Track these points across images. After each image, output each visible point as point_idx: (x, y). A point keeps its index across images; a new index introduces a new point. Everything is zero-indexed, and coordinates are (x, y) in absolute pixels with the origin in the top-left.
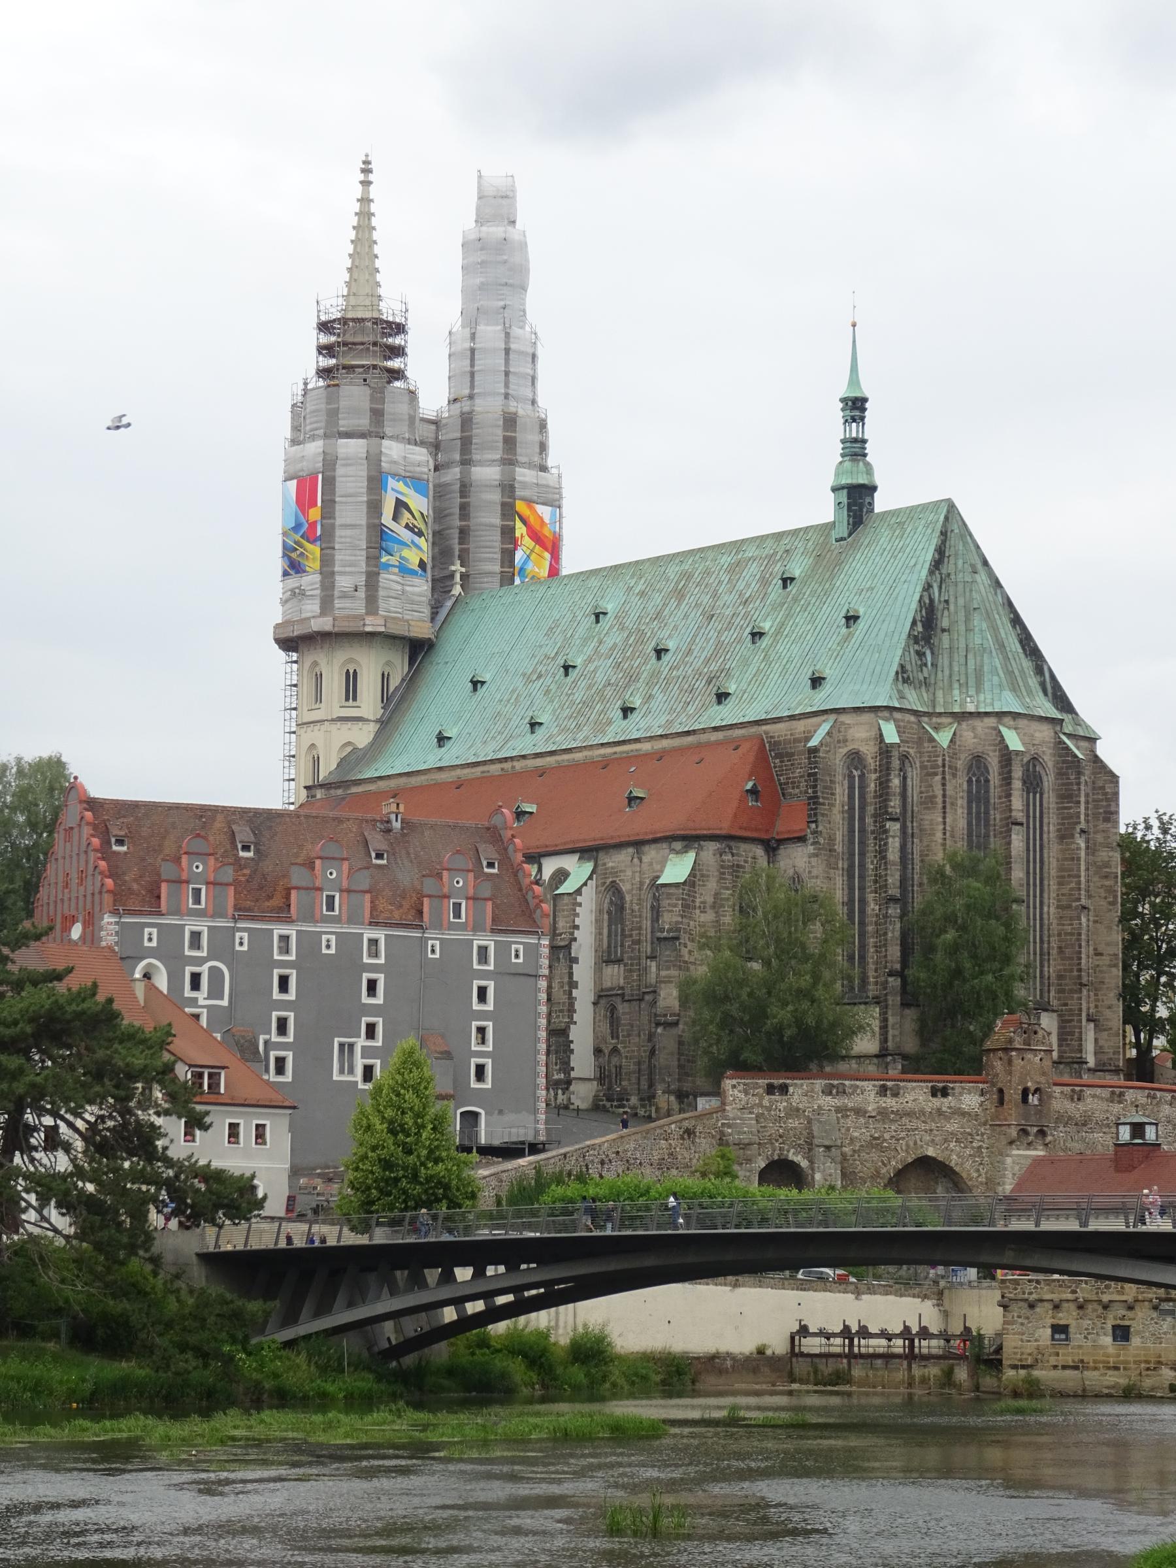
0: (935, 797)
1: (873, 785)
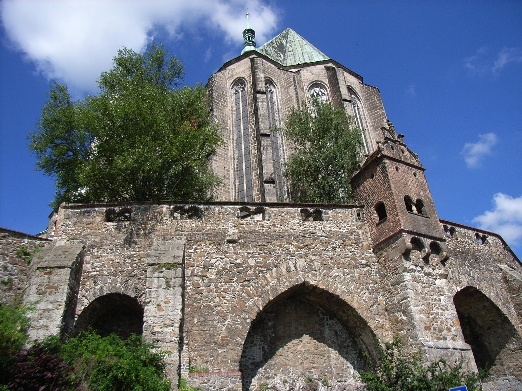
0: (292, 97)
1: (249, 89)
